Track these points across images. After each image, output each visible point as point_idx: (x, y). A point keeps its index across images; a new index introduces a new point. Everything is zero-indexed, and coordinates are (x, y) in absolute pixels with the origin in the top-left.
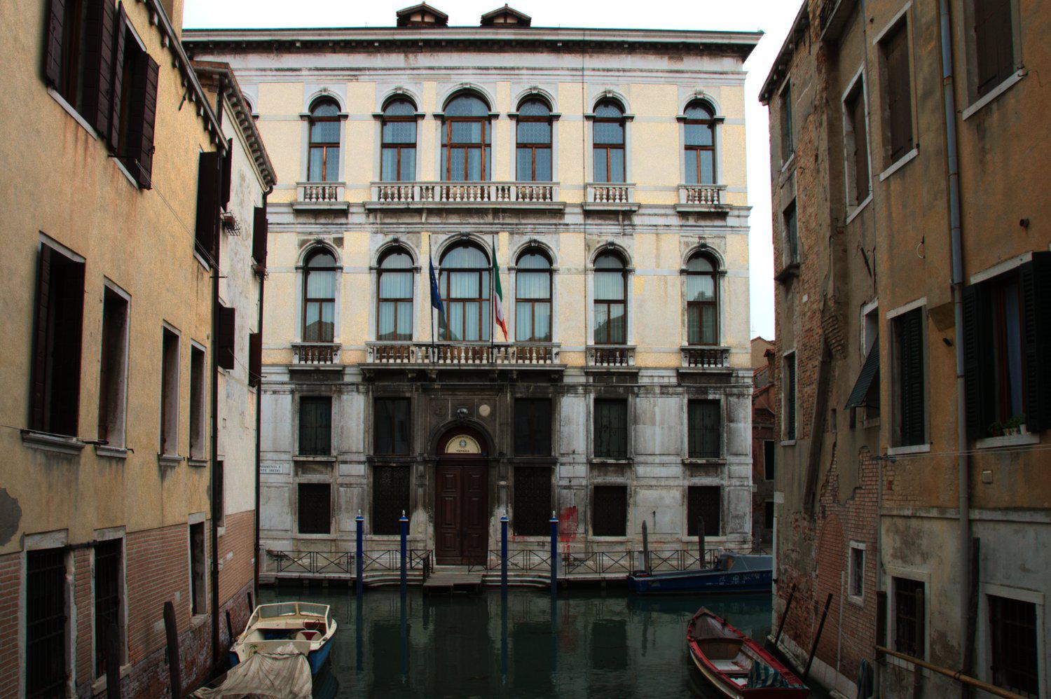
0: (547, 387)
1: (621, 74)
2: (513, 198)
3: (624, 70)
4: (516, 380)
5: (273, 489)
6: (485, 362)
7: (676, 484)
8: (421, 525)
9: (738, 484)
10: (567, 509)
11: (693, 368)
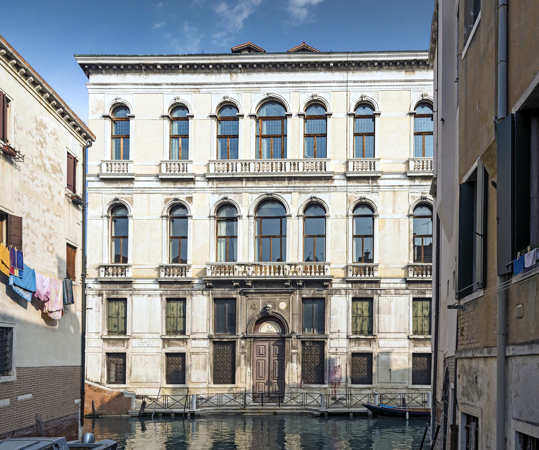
1: (373, 84)
2: (301, 170)
3: (374, 81)
4: (303, 286)
5: (148, 356)
6: (281, 274)
7: (404, 351)
11: (416, 278)
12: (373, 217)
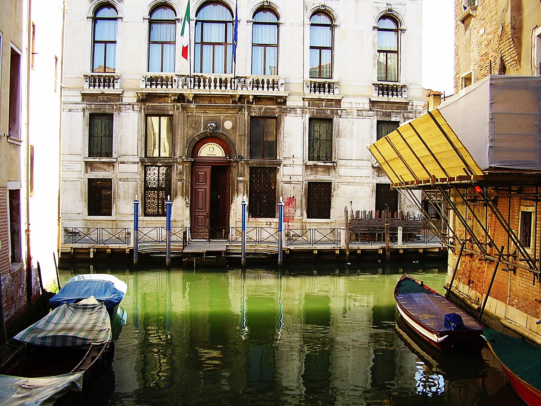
0: (274, 109)
5: (68, 182)
8: (180, 209)
10: (288, 199)
12: (332, 26)
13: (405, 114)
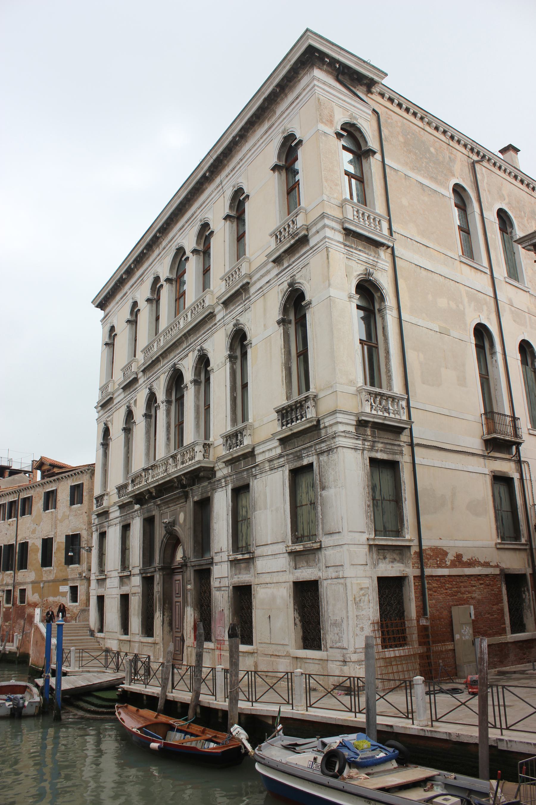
9: (334, 575)
13: (317, 447)
